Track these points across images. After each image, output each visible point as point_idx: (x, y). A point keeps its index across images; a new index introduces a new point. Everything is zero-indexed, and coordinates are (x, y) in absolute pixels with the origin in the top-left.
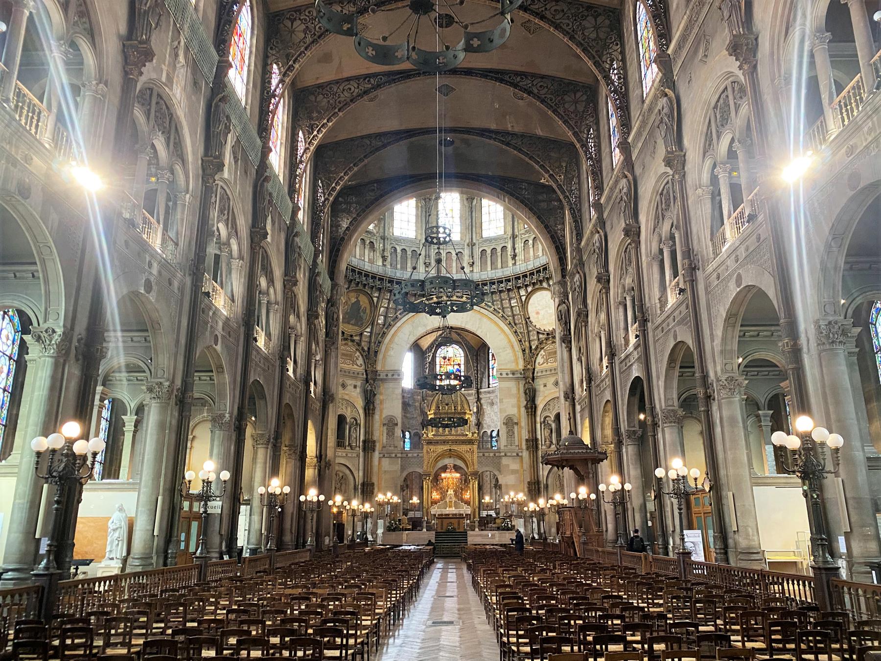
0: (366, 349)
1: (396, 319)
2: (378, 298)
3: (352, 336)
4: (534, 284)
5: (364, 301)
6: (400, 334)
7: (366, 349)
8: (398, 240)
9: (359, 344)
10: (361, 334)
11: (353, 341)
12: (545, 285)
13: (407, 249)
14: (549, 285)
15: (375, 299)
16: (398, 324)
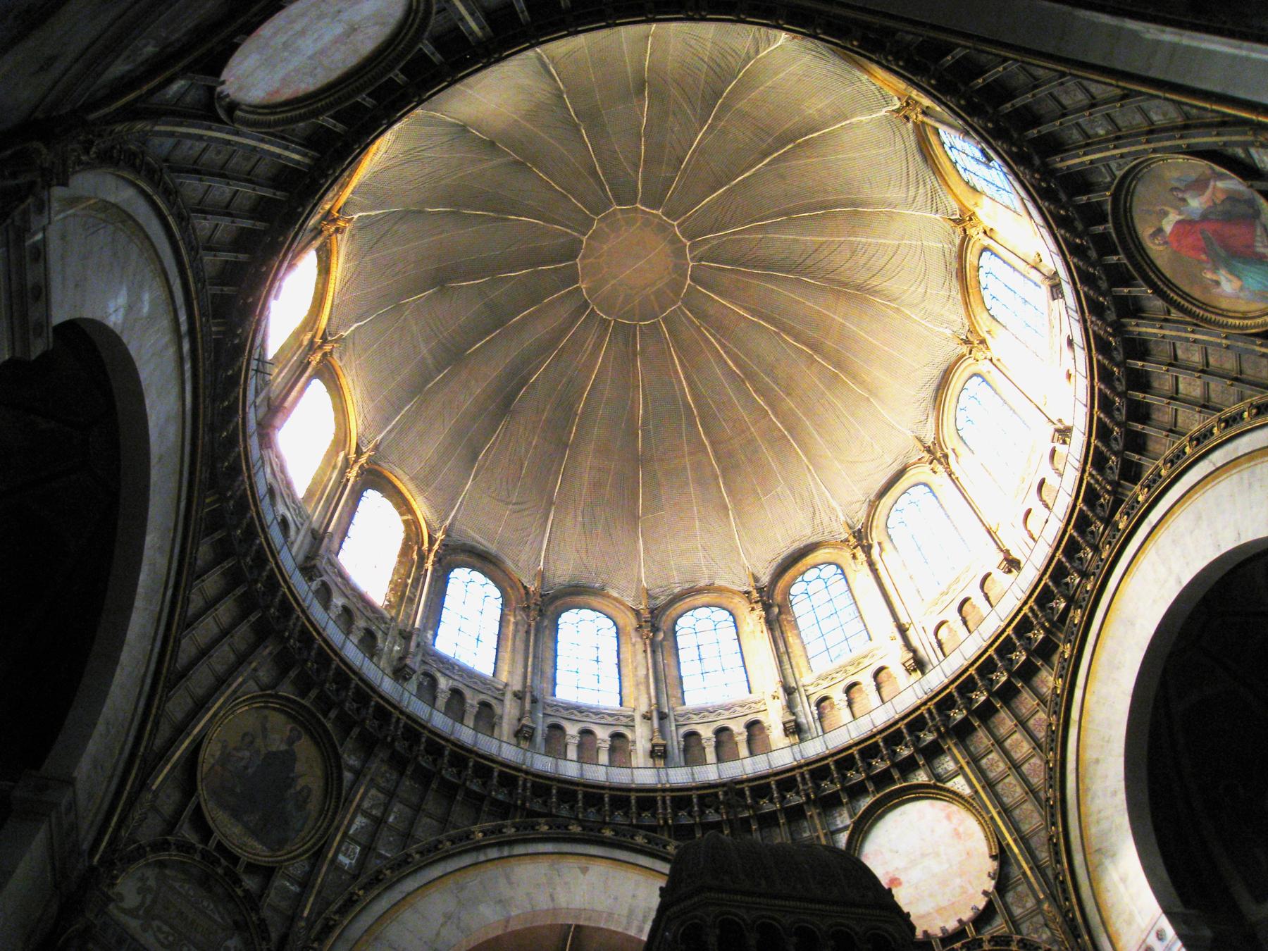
0: (274, 936)
1: (403, 867)
2: (358, 774)
3: (235, 859)
4: (883, 779)
5: (308, 771)
6: (408, 916)
7: (274, 936)
8: (448, 665)
9: (253, 901)
10: (268, 873)
11: (238, 881)
12: (922, 777)
13: (468, 694)
14: (939, 778)
15: (348, 776)
16: (410, 884)
